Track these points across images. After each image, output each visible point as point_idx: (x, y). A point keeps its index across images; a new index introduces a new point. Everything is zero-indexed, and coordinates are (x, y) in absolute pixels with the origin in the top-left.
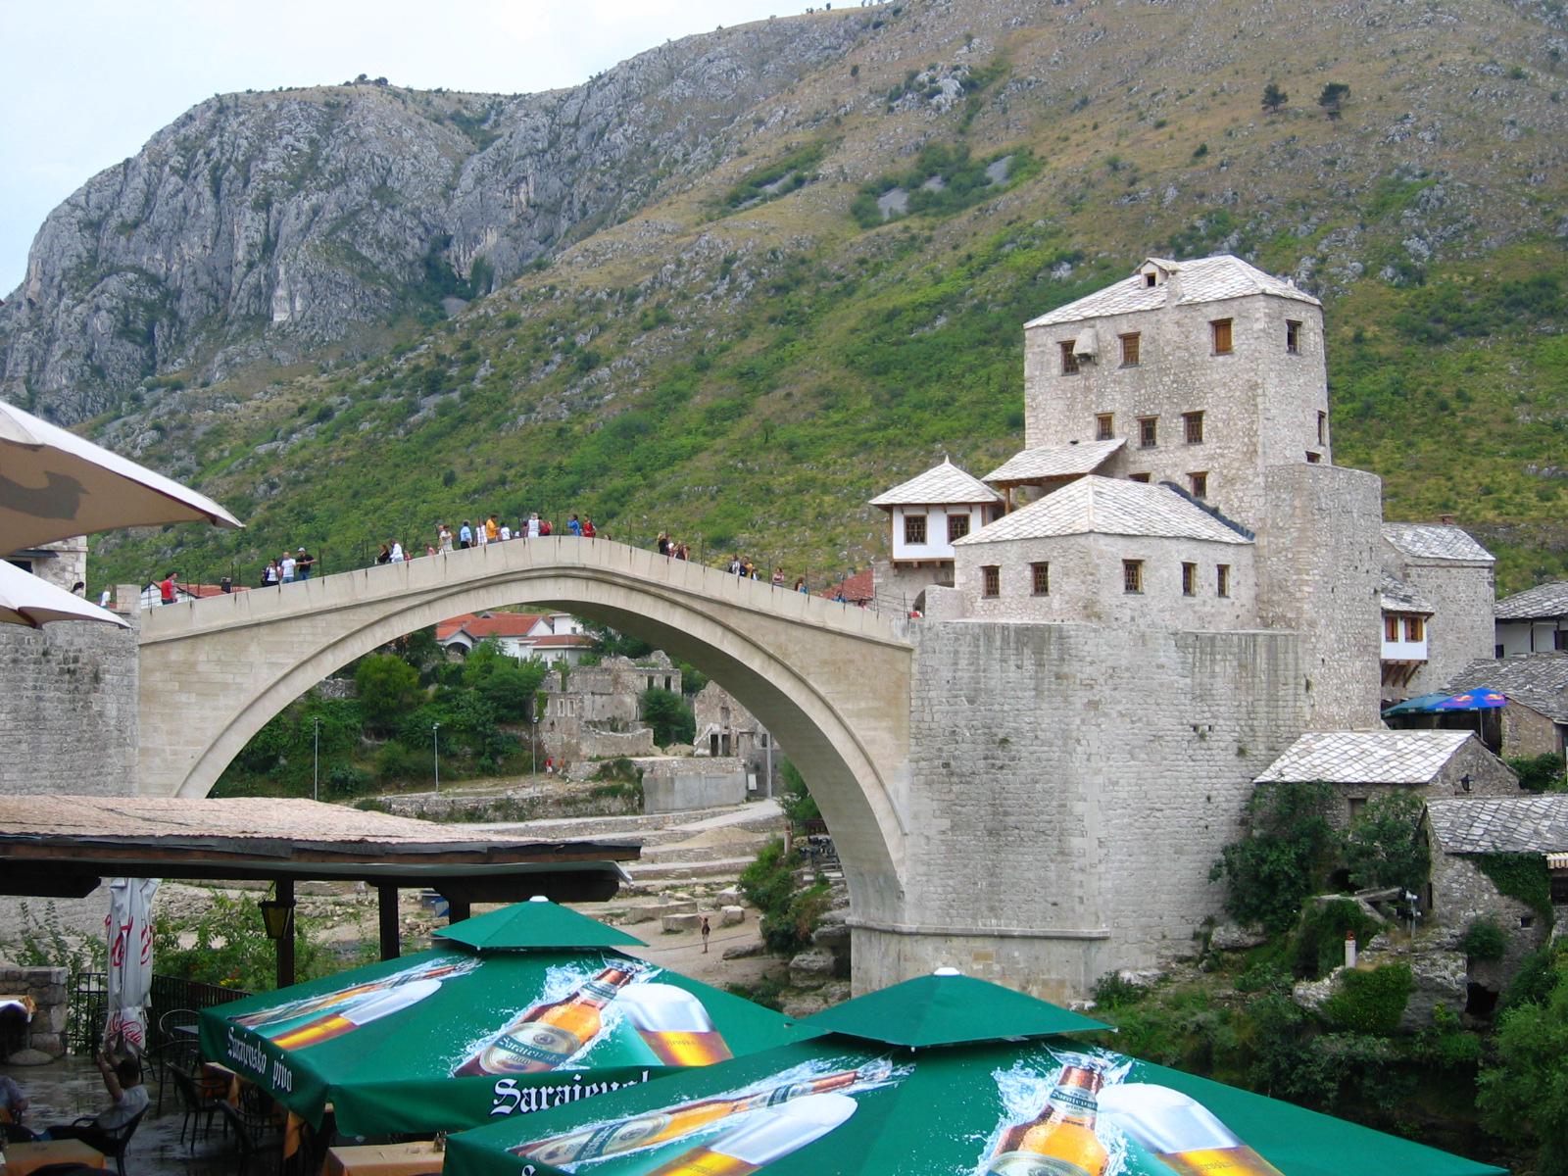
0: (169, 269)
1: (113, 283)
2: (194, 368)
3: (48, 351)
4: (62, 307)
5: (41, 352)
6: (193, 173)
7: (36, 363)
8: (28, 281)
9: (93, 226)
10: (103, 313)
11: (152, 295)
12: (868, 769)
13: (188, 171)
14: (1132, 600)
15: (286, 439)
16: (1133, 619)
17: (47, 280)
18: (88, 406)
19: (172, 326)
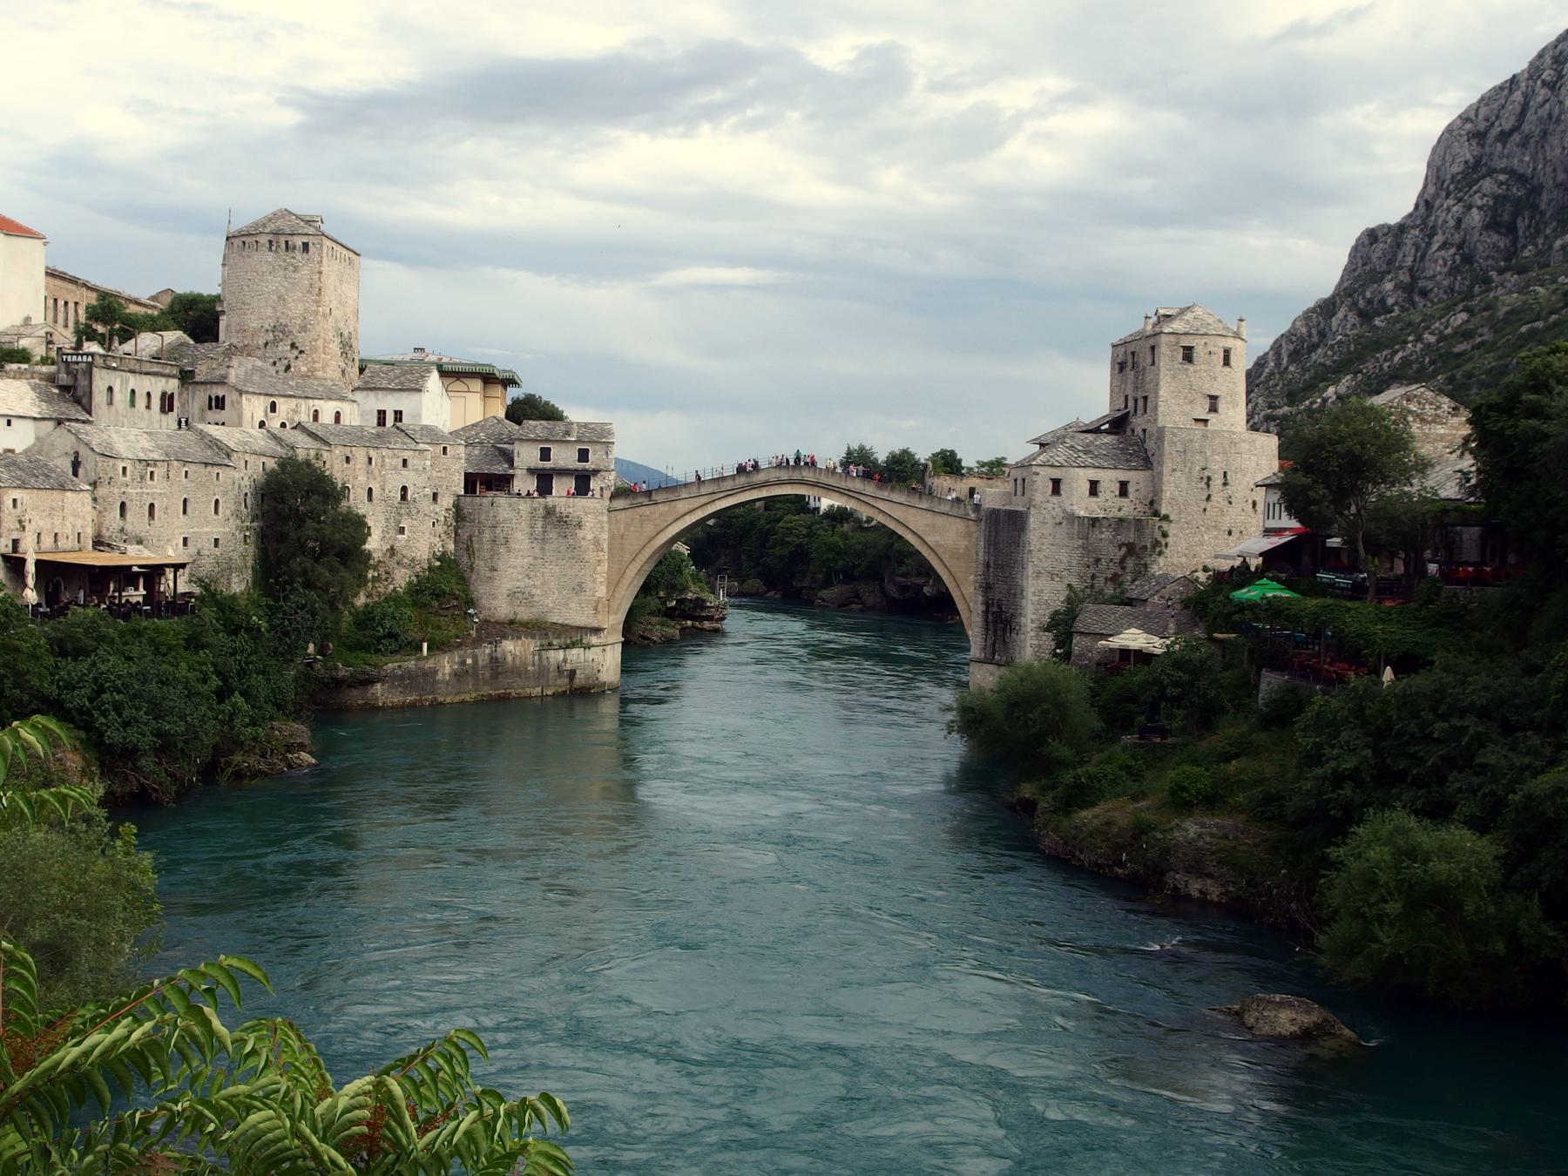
0: (1535, 169)
1: (1487, 185)
2: (1540, 253)
3: (1429, 245)
4: (1445, 206)
5: (1424, 245)
6: (1559, 85)
7: (1419, 254)
8: (1425, 187)
9: (1479, 136)
10: (1474, 210)
11: (1518, 192)
12: (952, 579)
13: (1556, 82)
14: (1055, 499)
15: (1545, 319)
16: (1054, 508)
17: (1438, 186)
18: (1457, 288)
19: (1532, 218)
